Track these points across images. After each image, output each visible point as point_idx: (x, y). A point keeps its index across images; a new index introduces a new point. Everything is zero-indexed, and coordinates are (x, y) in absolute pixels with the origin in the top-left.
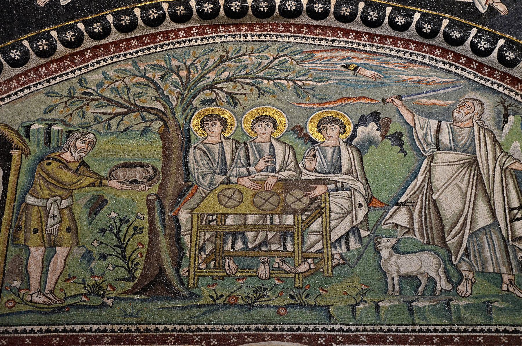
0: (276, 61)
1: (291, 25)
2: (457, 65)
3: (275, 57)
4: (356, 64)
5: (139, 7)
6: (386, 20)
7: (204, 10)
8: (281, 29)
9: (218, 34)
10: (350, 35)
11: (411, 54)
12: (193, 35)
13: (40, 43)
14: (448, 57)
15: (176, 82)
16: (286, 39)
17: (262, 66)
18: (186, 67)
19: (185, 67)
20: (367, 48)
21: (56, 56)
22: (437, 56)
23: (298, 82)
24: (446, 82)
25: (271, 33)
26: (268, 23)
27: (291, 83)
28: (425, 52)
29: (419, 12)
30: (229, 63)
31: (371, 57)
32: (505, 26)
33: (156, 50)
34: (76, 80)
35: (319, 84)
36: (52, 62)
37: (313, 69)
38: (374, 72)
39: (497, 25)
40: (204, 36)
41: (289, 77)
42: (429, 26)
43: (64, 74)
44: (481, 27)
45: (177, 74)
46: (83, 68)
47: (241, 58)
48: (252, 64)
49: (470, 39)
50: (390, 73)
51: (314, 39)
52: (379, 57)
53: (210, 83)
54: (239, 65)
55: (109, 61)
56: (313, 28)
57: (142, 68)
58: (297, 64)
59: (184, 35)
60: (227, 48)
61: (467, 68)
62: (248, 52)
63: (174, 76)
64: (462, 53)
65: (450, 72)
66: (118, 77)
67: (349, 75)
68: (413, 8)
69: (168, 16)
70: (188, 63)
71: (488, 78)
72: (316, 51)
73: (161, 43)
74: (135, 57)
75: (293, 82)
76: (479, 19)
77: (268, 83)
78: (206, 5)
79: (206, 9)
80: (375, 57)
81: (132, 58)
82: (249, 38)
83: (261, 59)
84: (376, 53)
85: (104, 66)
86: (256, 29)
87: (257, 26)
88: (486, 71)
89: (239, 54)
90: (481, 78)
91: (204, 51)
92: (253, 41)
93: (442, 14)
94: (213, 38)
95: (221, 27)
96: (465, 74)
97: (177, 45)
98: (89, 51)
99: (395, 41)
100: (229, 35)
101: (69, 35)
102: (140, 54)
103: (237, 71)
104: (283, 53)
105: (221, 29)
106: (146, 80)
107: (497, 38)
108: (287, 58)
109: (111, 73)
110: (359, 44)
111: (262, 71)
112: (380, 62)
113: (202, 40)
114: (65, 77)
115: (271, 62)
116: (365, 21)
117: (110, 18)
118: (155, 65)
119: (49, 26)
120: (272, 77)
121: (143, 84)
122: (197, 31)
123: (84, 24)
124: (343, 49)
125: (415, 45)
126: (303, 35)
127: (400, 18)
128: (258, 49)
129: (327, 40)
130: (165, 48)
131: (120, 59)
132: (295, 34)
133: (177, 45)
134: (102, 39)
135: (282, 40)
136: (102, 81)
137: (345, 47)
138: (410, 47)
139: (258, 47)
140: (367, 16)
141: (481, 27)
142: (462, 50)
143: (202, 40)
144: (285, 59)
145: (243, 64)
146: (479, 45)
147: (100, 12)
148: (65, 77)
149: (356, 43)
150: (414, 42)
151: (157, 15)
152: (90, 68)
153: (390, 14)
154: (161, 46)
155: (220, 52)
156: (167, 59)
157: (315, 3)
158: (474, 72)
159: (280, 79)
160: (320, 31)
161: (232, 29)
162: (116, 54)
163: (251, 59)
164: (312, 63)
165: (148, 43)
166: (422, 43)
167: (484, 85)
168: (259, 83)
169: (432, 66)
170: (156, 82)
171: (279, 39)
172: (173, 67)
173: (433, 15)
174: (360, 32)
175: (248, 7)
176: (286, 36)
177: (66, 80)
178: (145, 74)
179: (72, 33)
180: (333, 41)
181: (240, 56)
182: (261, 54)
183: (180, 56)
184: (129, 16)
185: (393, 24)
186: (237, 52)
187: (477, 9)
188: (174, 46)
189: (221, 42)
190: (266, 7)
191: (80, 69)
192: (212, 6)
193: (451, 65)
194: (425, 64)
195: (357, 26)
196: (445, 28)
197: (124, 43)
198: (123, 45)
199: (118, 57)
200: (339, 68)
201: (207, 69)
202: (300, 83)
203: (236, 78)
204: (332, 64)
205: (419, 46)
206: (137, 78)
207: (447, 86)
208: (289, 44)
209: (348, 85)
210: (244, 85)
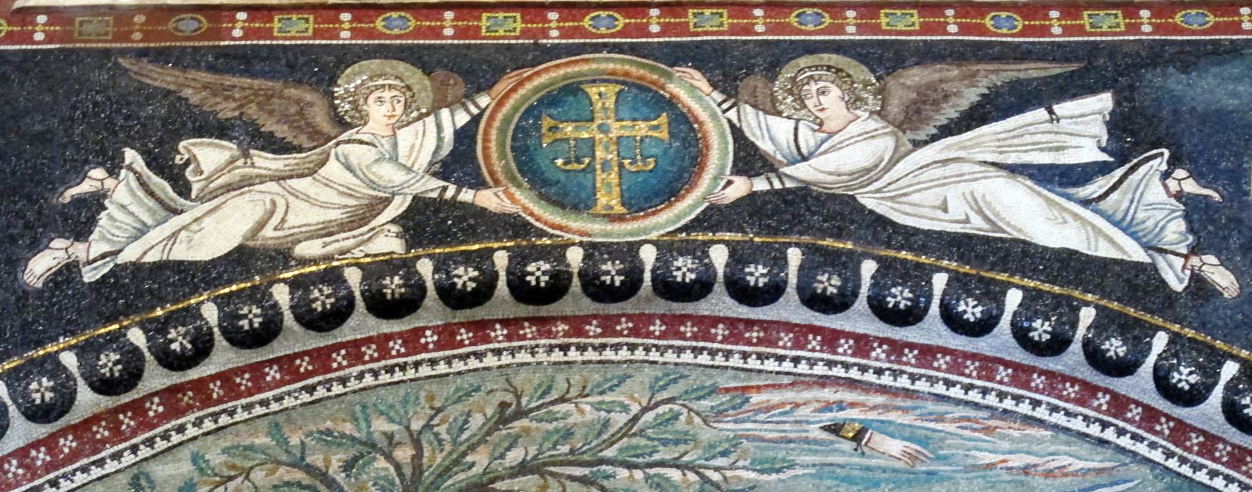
0: (649, 417)
1: (683, 319)
2: (1121, 424)
3: (644, 404)
4: (861, 421)
5: (284, 281)
6: (935, 309)
7: (455, 284)
8: (657, 328)
9: (491, 346)
10: (842, 346)
11: (1002, 396)
12: (425, 348)
13: (34, 386)
14: (1096, 403)
15: (386, 478)
16: (670, 357)
17: (612, 430)
18: (411, 435)
19: (406, 434)
20: (886, 380)
21: (73, 417)
22: (1067, 400)
23: (710, 474)
24: (1094, 470)
25: (632, 340)
26: (623, 315)
27: (692, 477)
28: (1037, 390)
29: (1018, 287)
30: (524, 422)
31: (899, 402)
32: (1236, 327)
33: (329, 390)
34: (124, 479)
35: (765, 477)
36: (63, 432)
37: (747, 438)
38: (906, 443)
39: (1216, 325)
40: (456, 352)
41: (686, 459)
42: (1047, 323)
43: (93, 463)
44: (1176, 328)
45: (389, 457)
46: (142, 447)
47: (555, 408)
48: (584, 424)
49: (1151, 360)
50: (949, 446)
51: (745, 356)
52: (919, 403)
53: (474, 480)
54: (550, 427)
55: (209, 425)
56: (741, 327)
57: (295, 440)
58: (705, 421)
59: (403, 350)
60: (517, 381)
61: (1145, 435)
62: (574, 392)
63: (381, 463)
64: (1132, 395)
65: (1103, 442)
66: (233, 467)
67: (843, 453)
68: (1003, 277)
69: (360, 304)
70: (416, 425)
71: (1200, 460)
72: (752, 387)
73: (341, 373)
74: (275, 413)
75: (698, 473)
76: (1171, 306)
77: (631, 476)
78: (460, 271)
79: (459, 282)
80: (909, 403)
81: (267, 415)
82: (573, 355)
83: (609, 412)
84: (908, 393)
85: (195, 438)
86: (593, 328)
87: (595, 322)
88: (1195, 441)
89: (548, 399)
90: (1183, 461)
91: (457, 390)
92: (584, 363)
93: (1076, 294)
94: (479, 356)
95: (498, 326)
96: (1142, 449)
97: (385, 378)
98: (156, 400)
99: (958, 360)
100: (521, 348)
101: (109, 362)
102: (288, 402)
103: (548, 445)
104: (665, 395)
105: (500, 332)
106: (308, 473)
107: (1219, 358)
108: (676, 407)
109: (215, 458)
110: (864, 369)
111: (613, 444)
112: (921, 417)
113: (449, 361)
114: (96, 472)
115: (636, 419)
116: (880, 310)
117: (211, 313)
118: (329, 432)
119: (54, 339)
120: (640, 460)
121: (299, 484)
122: (435, 338)
123: (146, 331)
124: (823, 381)
125: (1010, 371)
126: (716, 346)
127: (971, 302)
128: (598, 385)
129: (780, 359)
130: (353, 385)
131: (237, 418)
132: (694, 344)
133: (385, 378)
134: (190, 367)
135: (661, 360)
136: (192, 479)
137: (827, 377)
138: (998, 378)
139: (597, 377)
140: (885, 297)
141: (1176, 328)
142: (1134, 387)
143: (449, 361)
144: (671, 410)
145: (561, 424)
146: (1176, 375)
147: (186, 297)
148: (96, 472)
149: (855, 364)
150: (1007, 364)
151: (333, 300)
152: (161, 445)
153: (945, 293)
154: (343, 381)
155: (498, 394)
156: (359, 415)
157: (748, 263)
158: (1164, 443)
159: (662, 464)
160: (762, 334)
161: (529, 330)
162: (224, 406)
163: (582, 412)
164: (743, 421)
165: (309, 374)
166: (1028, 366)
167: (1191, 480)
168: (607, 477)
169: (1055, 427)
170: (334, 480)
171: (654, 356)
172: (377, 436)
173: (1055, 296)
174: (865, 336)
175: (570, 275)
176: (671, 347)
177: (99, 479)
178: (303, 458)
179: (115, 357)
180: (796, 360)
181: (553, 403)
182: (607, 398)
183: (392, 406)
184: (259, 304)
185: (953, 320)
186: (545, 393)
187: (1163, 283)
188: (376, 379)
189: (500, 367)
190: (619, 273)
191: (134, 449)
192: (476, 273)
193: (1105, 425)
194: (1041, 423)
195: (858, 319)
196: (1089, 328)
197: (247, 376)
198: (244, 381)
199: (231, 413)
200: (815, 432)
201: (467, 440)
202: (715, 477)
203: (545, 464)
204: (797, 422)
205: (1021, 374)
206: (282, 470)
207: (1098, 480)
208: (681, 369)
209: (843, 480)
210: (568, 483)
